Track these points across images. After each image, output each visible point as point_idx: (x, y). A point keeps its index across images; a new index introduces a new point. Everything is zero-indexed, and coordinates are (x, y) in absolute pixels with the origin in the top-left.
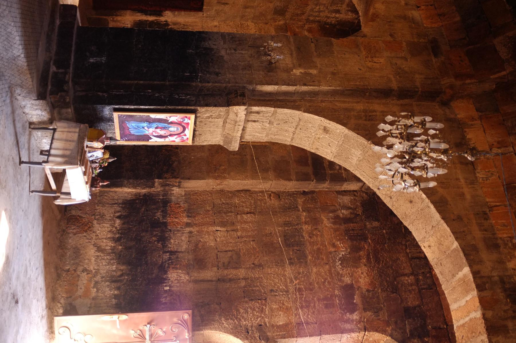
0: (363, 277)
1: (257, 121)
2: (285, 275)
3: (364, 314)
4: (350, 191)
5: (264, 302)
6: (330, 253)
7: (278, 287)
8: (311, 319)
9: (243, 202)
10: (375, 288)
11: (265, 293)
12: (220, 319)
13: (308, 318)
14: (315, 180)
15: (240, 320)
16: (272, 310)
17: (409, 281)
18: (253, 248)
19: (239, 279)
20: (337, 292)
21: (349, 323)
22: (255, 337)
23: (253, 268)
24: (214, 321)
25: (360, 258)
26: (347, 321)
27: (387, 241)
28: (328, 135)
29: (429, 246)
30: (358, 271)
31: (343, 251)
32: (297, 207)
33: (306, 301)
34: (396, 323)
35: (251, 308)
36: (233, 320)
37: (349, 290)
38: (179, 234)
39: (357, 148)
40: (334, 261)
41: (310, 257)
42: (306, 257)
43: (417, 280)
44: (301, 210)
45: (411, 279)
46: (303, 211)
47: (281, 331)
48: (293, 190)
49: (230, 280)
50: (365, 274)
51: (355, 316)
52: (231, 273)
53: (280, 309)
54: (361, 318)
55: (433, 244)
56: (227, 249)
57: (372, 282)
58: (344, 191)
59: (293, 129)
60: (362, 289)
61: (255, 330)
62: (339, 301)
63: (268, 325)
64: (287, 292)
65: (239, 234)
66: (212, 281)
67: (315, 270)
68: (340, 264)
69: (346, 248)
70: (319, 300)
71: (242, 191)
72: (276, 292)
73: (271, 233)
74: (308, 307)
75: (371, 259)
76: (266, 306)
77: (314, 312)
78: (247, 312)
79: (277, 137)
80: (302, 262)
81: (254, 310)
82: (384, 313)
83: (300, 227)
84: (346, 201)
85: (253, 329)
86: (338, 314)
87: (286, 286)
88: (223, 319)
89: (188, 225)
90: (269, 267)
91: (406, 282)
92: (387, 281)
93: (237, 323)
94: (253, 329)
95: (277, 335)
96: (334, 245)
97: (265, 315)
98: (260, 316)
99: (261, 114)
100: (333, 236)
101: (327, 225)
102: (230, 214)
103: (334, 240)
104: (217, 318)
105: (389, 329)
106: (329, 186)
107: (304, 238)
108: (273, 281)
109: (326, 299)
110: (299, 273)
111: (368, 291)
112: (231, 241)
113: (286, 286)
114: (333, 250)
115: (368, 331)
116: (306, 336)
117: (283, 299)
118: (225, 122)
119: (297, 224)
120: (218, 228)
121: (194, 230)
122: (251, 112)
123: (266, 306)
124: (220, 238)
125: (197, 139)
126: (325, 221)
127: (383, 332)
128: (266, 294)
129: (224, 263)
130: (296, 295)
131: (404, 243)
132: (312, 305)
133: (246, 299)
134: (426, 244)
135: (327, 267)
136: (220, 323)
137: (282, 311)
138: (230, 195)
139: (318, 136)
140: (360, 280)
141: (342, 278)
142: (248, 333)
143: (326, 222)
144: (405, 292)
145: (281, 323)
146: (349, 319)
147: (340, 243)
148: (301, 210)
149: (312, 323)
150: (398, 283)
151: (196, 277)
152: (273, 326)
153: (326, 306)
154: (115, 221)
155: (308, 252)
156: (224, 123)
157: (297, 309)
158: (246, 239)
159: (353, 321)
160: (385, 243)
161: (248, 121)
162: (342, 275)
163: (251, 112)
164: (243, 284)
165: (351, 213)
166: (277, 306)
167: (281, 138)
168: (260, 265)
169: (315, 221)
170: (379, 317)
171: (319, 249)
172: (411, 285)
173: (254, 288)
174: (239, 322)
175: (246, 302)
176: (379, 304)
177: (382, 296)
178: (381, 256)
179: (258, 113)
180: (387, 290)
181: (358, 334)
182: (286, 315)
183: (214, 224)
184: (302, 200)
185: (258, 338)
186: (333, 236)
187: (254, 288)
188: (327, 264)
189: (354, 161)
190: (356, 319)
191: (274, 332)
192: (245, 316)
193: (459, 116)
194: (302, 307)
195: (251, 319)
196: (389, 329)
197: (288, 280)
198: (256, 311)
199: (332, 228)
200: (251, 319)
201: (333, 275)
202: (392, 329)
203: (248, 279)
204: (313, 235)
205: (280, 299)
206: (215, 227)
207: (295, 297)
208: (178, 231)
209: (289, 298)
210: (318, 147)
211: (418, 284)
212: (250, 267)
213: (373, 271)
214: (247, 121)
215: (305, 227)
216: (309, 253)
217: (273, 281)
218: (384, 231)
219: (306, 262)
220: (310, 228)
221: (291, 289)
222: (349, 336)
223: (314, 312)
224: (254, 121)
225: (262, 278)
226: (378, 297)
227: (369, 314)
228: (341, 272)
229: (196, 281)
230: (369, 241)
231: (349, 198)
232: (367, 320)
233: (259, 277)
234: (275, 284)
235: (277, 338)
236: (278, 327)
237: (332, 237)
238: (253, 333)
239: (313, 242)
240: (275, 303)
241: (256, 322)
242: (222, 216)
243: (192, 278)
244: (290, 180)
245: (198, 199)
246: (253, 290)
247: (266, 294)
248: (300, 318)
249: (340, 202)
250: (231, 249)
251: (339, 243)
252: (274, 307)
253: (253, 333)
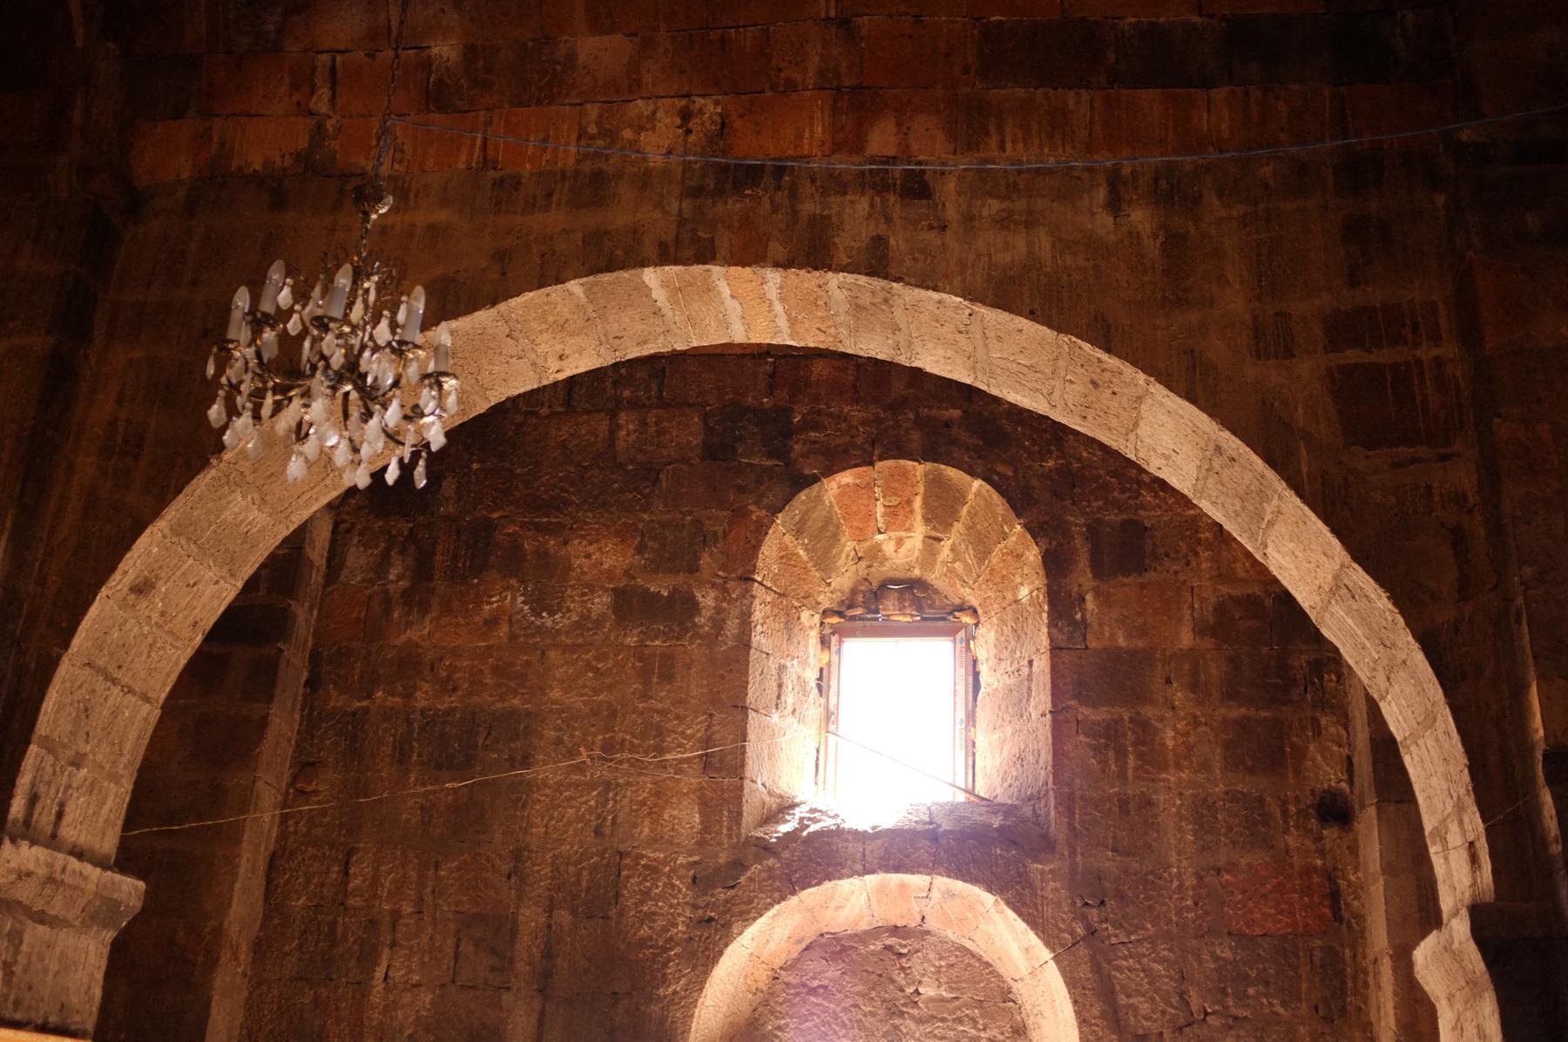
0: (600, 557)
1: (62, 805)
2: (559, 784)
3: (705, 574)
4: (333, 542)
5: (627, 861)
6: (513, 637)
7: (590, 810)
8: (697, 728)
9: (308, 882)
10: (636, 529)
11: (601, 855)
12: (660, 999)
13: (693, 736)
14: (281, 645)
15: (671, 939)
16: (655, 840)
17: (631, 427)
18: (459, 869)
19: (549, 926)
20: (631, 641)
21: (724, 621)
22: (727, 901)
23: (522, 881)
24: (663, 1020)
25: (542, 555)
26: (718, 624)
27: (507, 465)
28: (160, 583)
29: (561, 358)
30: (580, 567)
31: (514, 598)
32: (354, 714)
33: (644, 735)
34: (742, 490)
35: (642, 902)
36: (669, 960)
37: (631, 604)
39: (224, 502)
40: (540, 631)
41: (516, 701)
42: (513, 713)
43: (633, 404)
44: (365, 703)
45: (628, 423)
46: (369, 696)
47: (720, 822)
48: (297, 717)
49: (548, 955)
50: (591, 549)
51: (707, 600)
52: (526, 947)
53: (655, 815)
54: (714, 585)
55: (558, 348)
56: (450, 951)
57: (617, 533)
58: (329, 560)
59: (116, 690)
60: (632, 566)
61: (707, 898)
62: (657, 638)
63: (696, 858)
64: (608, 786)
65: (407, 908)
66: (542, 1014)
67: (556, 694)
68: (551, 613)
69: (507, 589)
70: (645, 697)
71: (268, 883)
72: (605, 819)
73: (422, 808)
74: (660, 733)
75: (550, 523)
76: (642, 857)
77: (678, 717)
78: (651, 916)
79: (128, 747)
80: (526, 727)
81: (646, 894)
82: (710, 519)
83: (418, 715)
84: (362, 562)
85: (702, 904)
86: (694, 648)
87: (591, 786)
88: (661, 992)
90: (526, 831)
91: (633, 437)
92: (621, 492)
93: (678, 950)
94: (702, 904)
95: (730, 837)
96: (492, 623)
97: (665, 863)
98: (669, 877)
99: (42, 789)
100: (461, 620)
101: (426, 631)
102: (340, 929)
103: (477, 619)
104: (655, 1008)
105: (757, 513)
106: (307, 605)
107: (454, 710)
108: (569, 823)
109: (644, 676)
110: (559, 741)
111: (640, 550)
112: (425, 938)
113: (591, 786)
114: (503, 630)
115: (753, 572)
116: (743, 751)
117: (626, 801)
118: (41, 918)
119: (408, 721)
120: (380, 973)
122: (27, 822)
123: (642, 857)
124: (410, 971)
125: (75, 1020)
126: (413, 634)
127: (761, 529)
128: (605, 850)
129: (493, 969)
130: (621, 762)
131: (519, 418)
132: (657, 718)
133: (613, 912)
134: (553, 364)
135: (552, 654)
136: (671, 1002)
137: (663, 809)
138: (276, 921)
139: (155, 617)
140: (606, 566)
141: (594, 616)
142: (711, 919)
143: (420, 632)
144: (659, 445)
145: (697, 818)
146: (711, 619)
147: (490, 603)
148: (365, 703)
149: (709, 727)
150: (632, 461)
152: (701, 844)
153: (667, 677)
155: (499, 705)
156: (42, 922)
157: (663, 766)
158: (429, 889)
159: (719, 610)
160: (511, 471)
161: (54, 836)
162: (585, 617)
163: (27, 822)
164: (564, 916)
165: (402, 553)
166: (647, 823)
167: (132, 735)
168: (517, 856)
169: (410, 665)
170: (720, 534)
171: (495, 670)
172: (644, 423)
173: (584, 884)
174: (678, 944)
175: (621, 913)
176: (683, 526)
177: (664, 513)
178: (546, 492)
179: (33, 799)
180: (644, 496)
181: (757, 602)
182: (674, 800)
183: (363, 987)
184: (334, 693)
185: (731, 893)
186: (461, 620)
187: (584, 884)
188: (543, 653)
189: (259, 517)
190: (716, 599)
191: (720, 844)
192: (660, 923)
193: (185, 175)
194: (660, 750)
195: (671, 906)
196: (757, 513)
197: (575, 777)
198: (650, 889)
199: (438, 619)
200: (671, 906)
201: (580, 641)
202: (755, 503)
203: (551, 899)
204: (449, 676)
205: (627, 810)
206: (374, 982)
207: (625, 766)
209: (629, 784)
210: (190, 620)
211: (644, 406)
212: (518, 890)
213: (586, 523)
214: (52, 841)
215: (421, 700)
216: (502, 700)
217: (569, 823)
218: (475, 466)
219: (529, 714)
220: (426, 686)
221: (601, 772)
222: (759, 628)
223: (678, 717)
224: (60, 815)
225: (555, 857)
226: (663, 526)
227: (705, 560)
228: (575, 618)
230: (496, 515)
231: (353, 549)
232: (724, 568)
233: (553, 863)
234: (580, 819)
235: (739, 835)
236: (706, 828)
237: (467, 624)
238: (714, 907)
239: (472, 684)
240: (635, 825)
241: (684, 892)
242: (342, 956)
244: (264, 722)
245: (272, 1031)
246: (588, 889)
247: (605, 850)
248: (688, 760)
249: (363, 581)
250: (451, 941)
252: (646, 831)
253: (714, 907)
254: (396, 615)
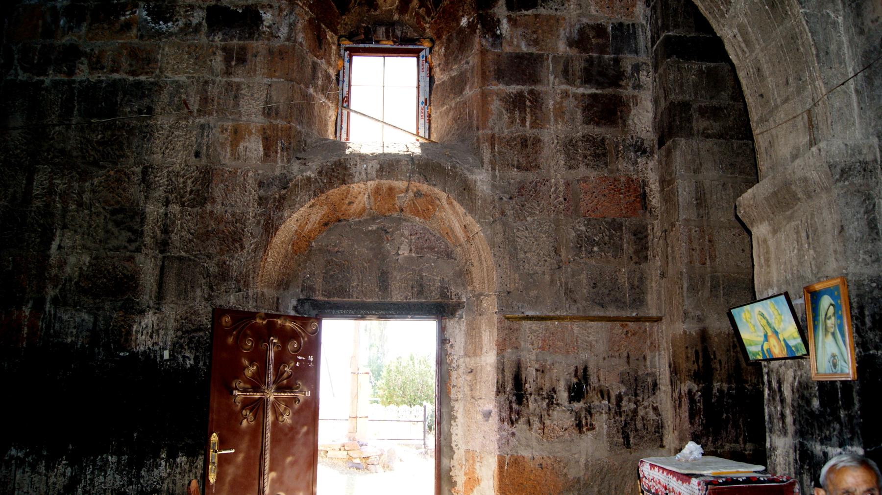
19: (166, 214)
38: (57, 325)
49: (166, 231)
64: (202, 127)
66: (162, 268)
68: (166, 22)
83: (77, 85)
86: (258, 45)
89: (39, 305)
107: (102, 81)
109: (227, 60)
120: (54, 246)
121: (51, 292)
145: (261, 149)
151: (150, 297)
154: (12, 457)
162: (188, 25)
169: (71, 55)
184: (20, 72)
186: (106, 26)
208: (48, 327)
229: (160, 297)
233: (168, 175)
243: (152, 304)
246: (191, 191)
251: (123, 18)
254: (62, 22)
